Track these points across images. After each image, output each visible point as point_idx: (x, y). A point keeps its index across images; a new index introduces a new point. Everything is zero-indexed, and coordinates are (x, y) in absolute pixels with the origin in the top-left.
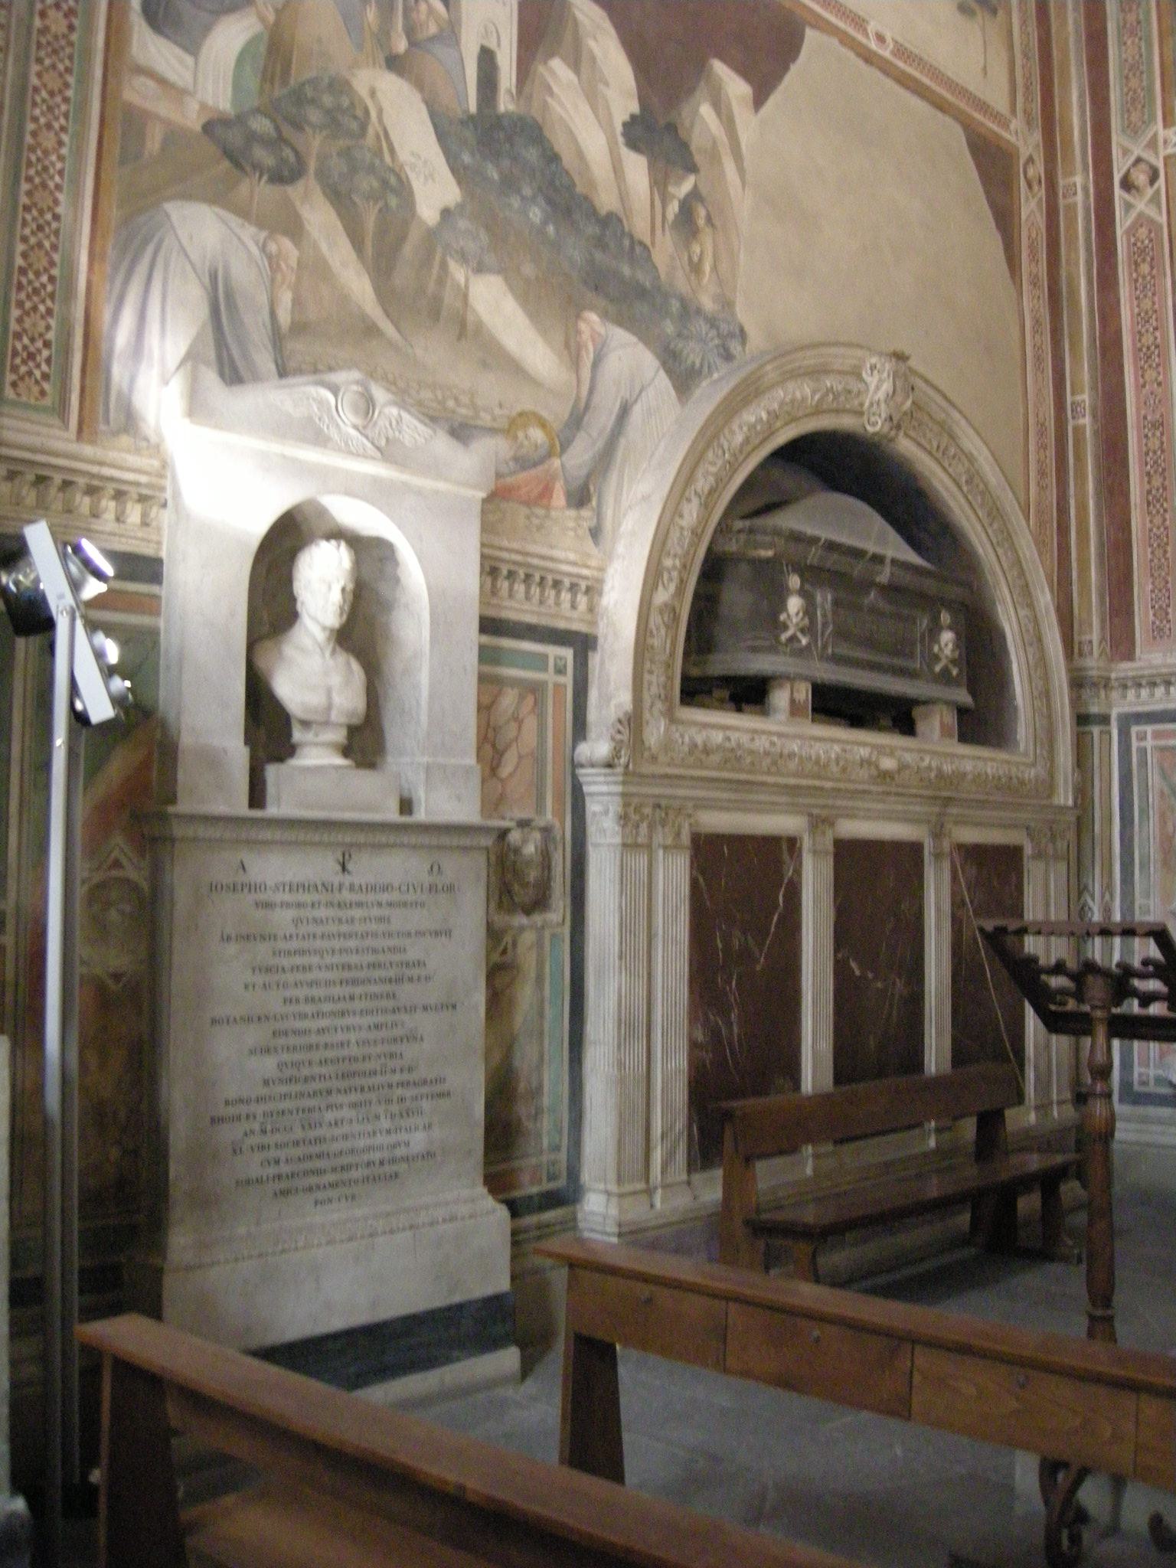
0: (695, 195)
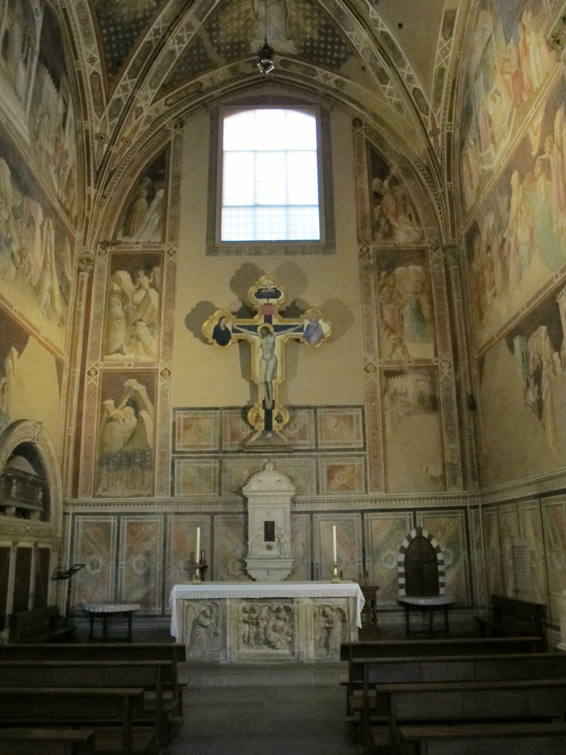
0: (5, 383)
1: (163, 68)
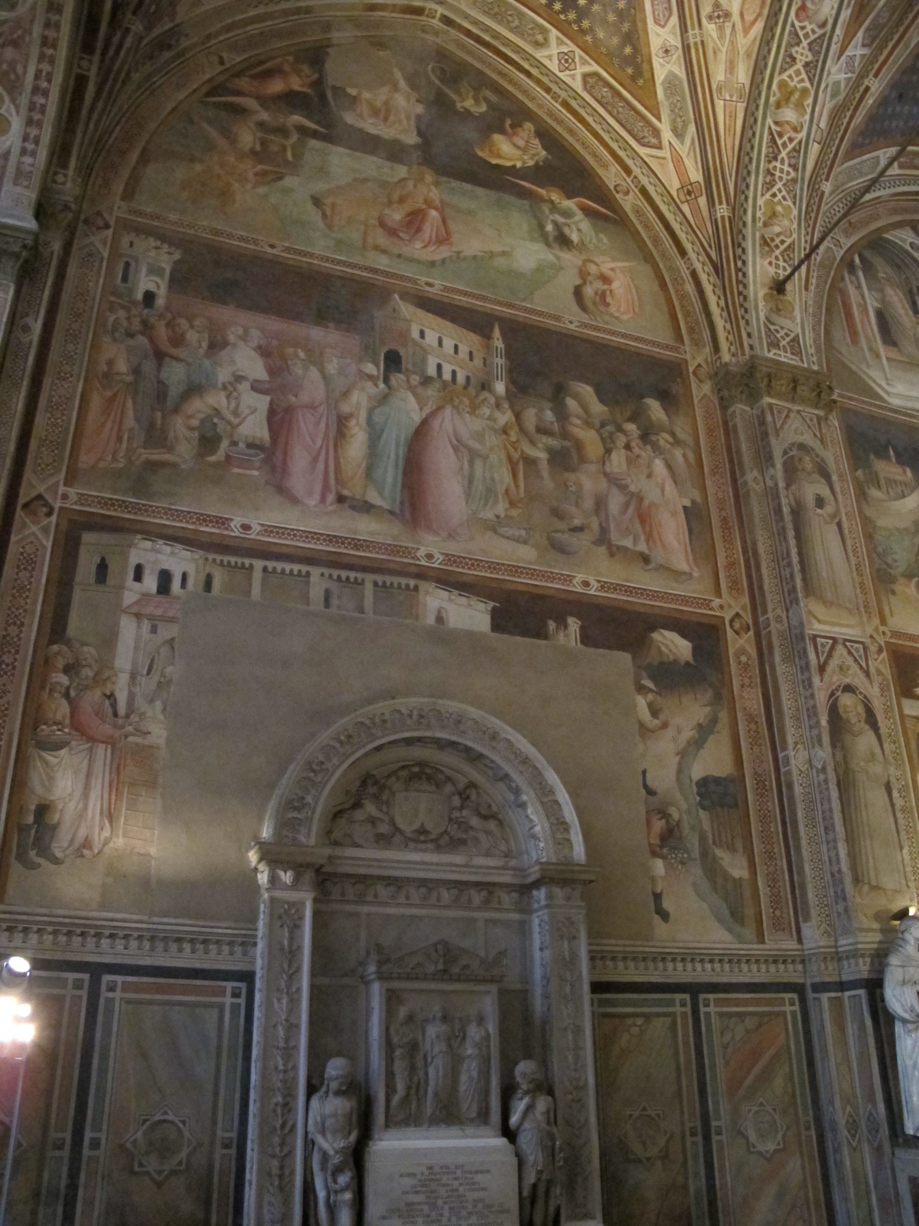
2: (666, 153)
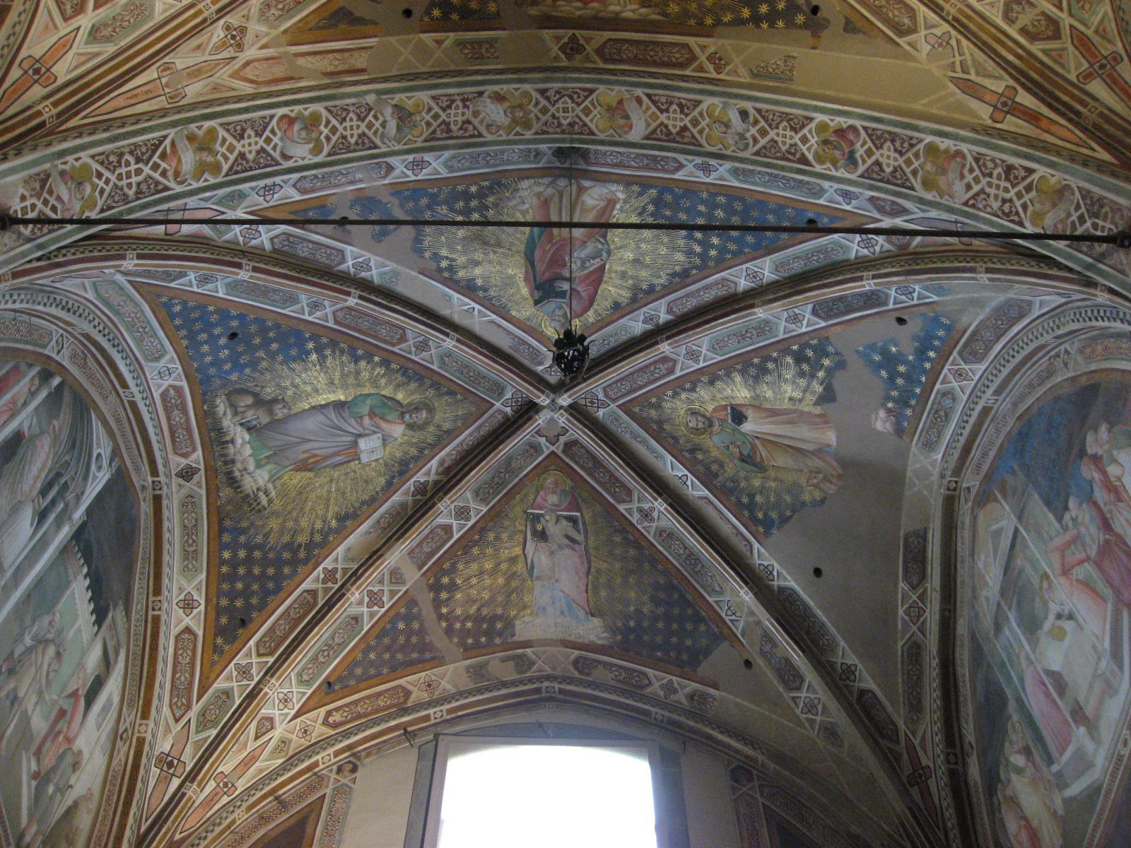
1: (331, 648)
2: (65, 29)
